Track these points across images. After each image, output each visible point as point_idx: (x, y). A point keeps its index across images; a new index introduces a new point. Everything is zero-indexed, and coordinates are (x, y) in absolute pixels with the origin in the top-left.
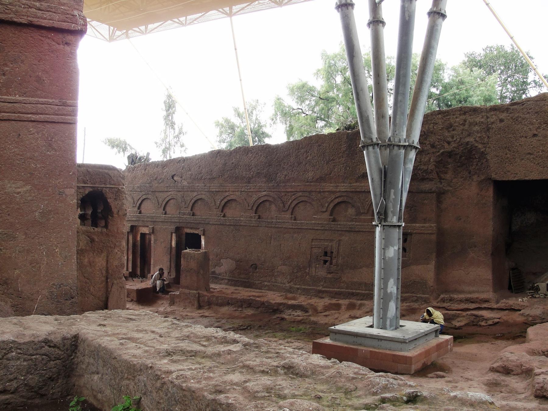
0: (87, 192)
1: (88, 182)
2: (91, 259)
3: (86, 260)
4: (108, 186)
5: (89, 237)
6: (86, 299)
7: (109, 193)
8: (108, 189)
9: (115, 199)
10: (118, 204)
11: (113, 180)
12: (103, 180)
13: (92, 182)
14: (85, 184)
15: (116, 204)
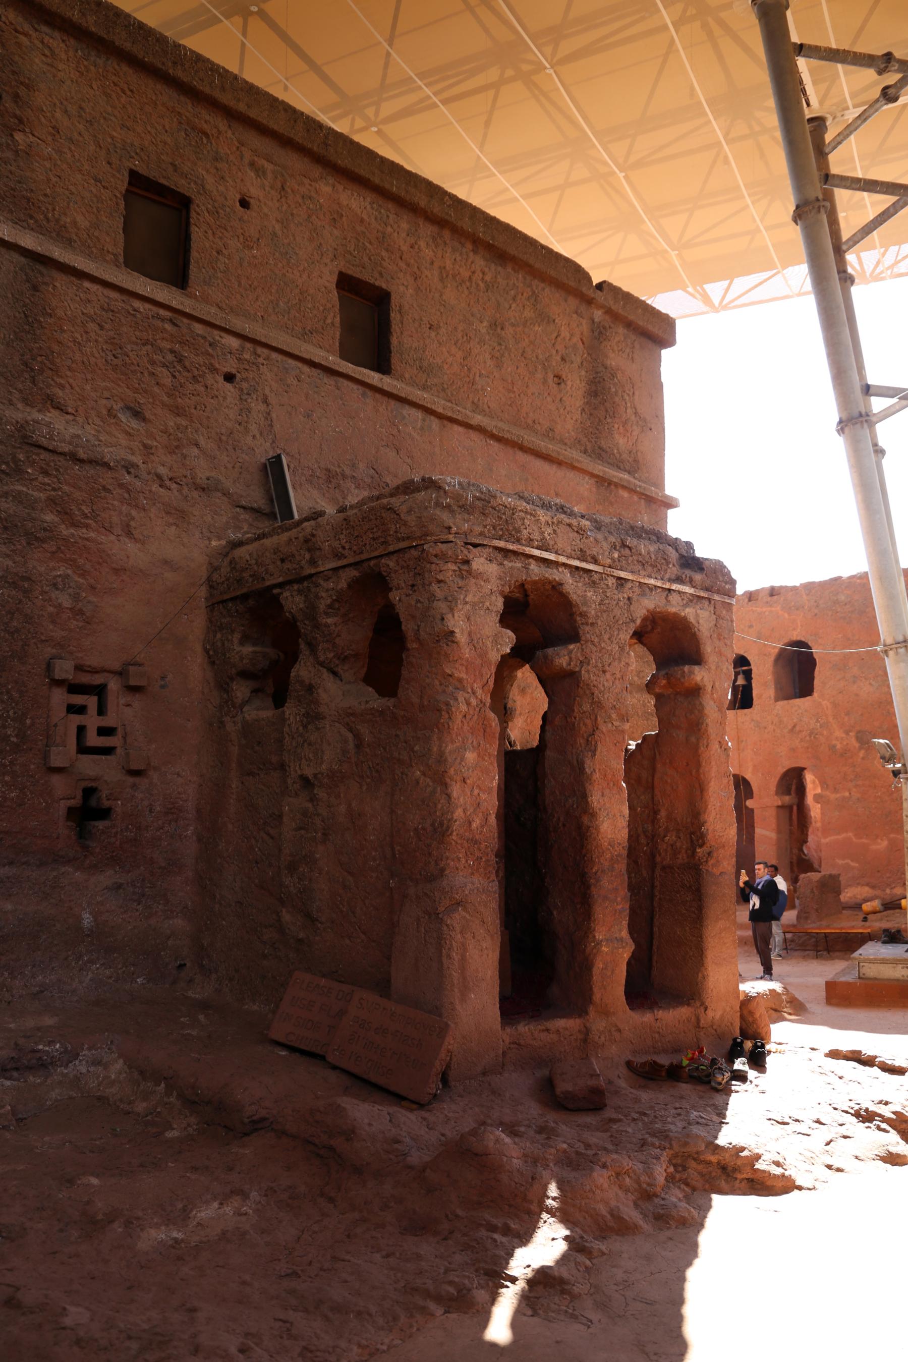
0: (343, 584)
1: (346, 552)
2: (354, 804)
3: (343, 808)
4: (391, 548)
5: (350, 730)
6: (347, 941)
7: (396, 572)
8: (394, 557)
9: (413, 586)
10: (418, 601)
11: (405, 524)
12: (379, 534)
13: (355, 548)
14: (339, 559)
15: (413, 603)
